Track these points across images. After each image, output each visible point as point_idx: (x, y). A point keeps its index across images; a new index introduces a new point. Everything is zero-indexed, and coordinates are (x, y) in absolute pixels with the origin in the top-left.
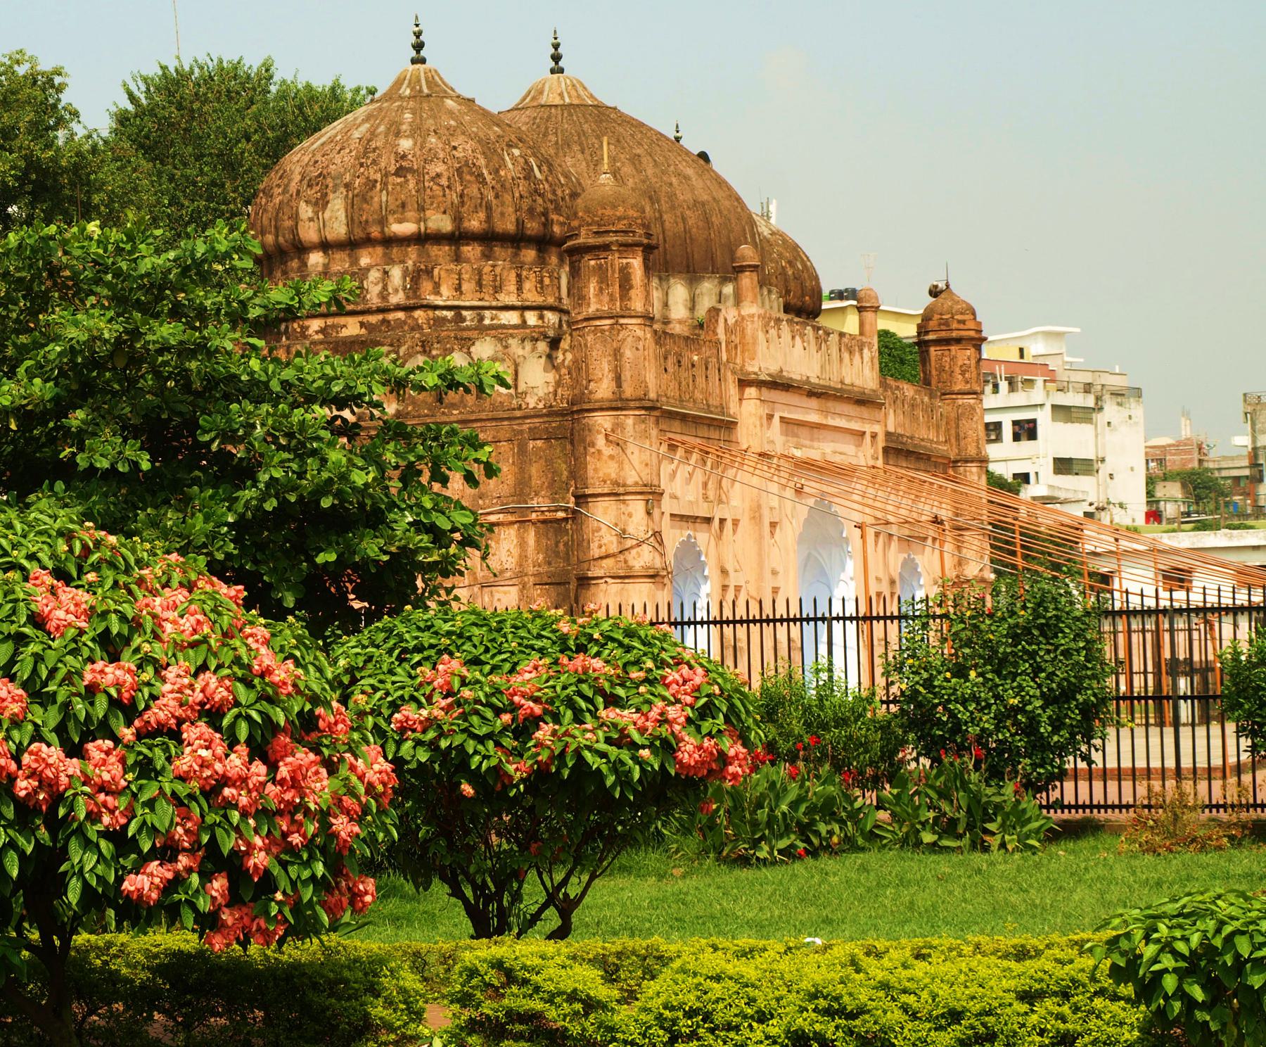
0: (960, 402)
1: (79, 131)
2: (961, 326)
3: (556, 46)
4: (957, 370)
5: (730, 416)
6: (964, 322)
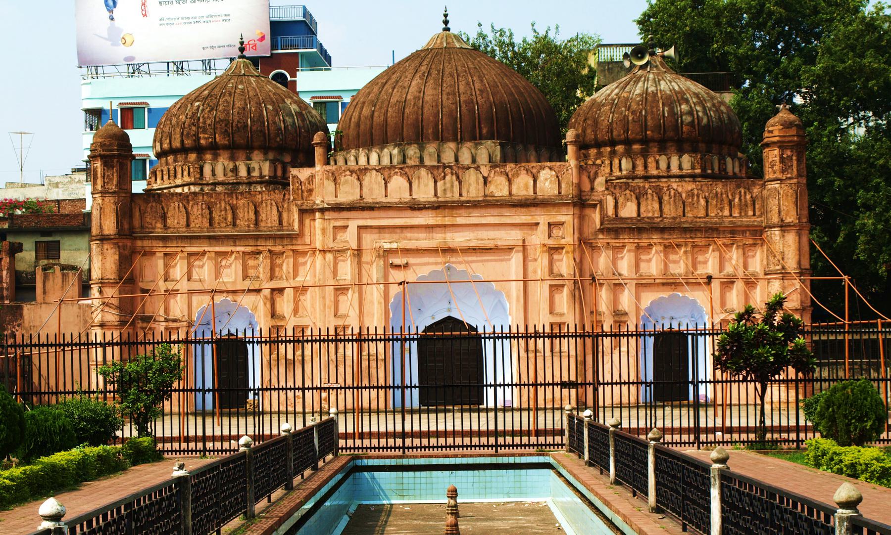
1: (347, 99)
2: (770, 135)
3: (446, 16)
5: (293, 230)
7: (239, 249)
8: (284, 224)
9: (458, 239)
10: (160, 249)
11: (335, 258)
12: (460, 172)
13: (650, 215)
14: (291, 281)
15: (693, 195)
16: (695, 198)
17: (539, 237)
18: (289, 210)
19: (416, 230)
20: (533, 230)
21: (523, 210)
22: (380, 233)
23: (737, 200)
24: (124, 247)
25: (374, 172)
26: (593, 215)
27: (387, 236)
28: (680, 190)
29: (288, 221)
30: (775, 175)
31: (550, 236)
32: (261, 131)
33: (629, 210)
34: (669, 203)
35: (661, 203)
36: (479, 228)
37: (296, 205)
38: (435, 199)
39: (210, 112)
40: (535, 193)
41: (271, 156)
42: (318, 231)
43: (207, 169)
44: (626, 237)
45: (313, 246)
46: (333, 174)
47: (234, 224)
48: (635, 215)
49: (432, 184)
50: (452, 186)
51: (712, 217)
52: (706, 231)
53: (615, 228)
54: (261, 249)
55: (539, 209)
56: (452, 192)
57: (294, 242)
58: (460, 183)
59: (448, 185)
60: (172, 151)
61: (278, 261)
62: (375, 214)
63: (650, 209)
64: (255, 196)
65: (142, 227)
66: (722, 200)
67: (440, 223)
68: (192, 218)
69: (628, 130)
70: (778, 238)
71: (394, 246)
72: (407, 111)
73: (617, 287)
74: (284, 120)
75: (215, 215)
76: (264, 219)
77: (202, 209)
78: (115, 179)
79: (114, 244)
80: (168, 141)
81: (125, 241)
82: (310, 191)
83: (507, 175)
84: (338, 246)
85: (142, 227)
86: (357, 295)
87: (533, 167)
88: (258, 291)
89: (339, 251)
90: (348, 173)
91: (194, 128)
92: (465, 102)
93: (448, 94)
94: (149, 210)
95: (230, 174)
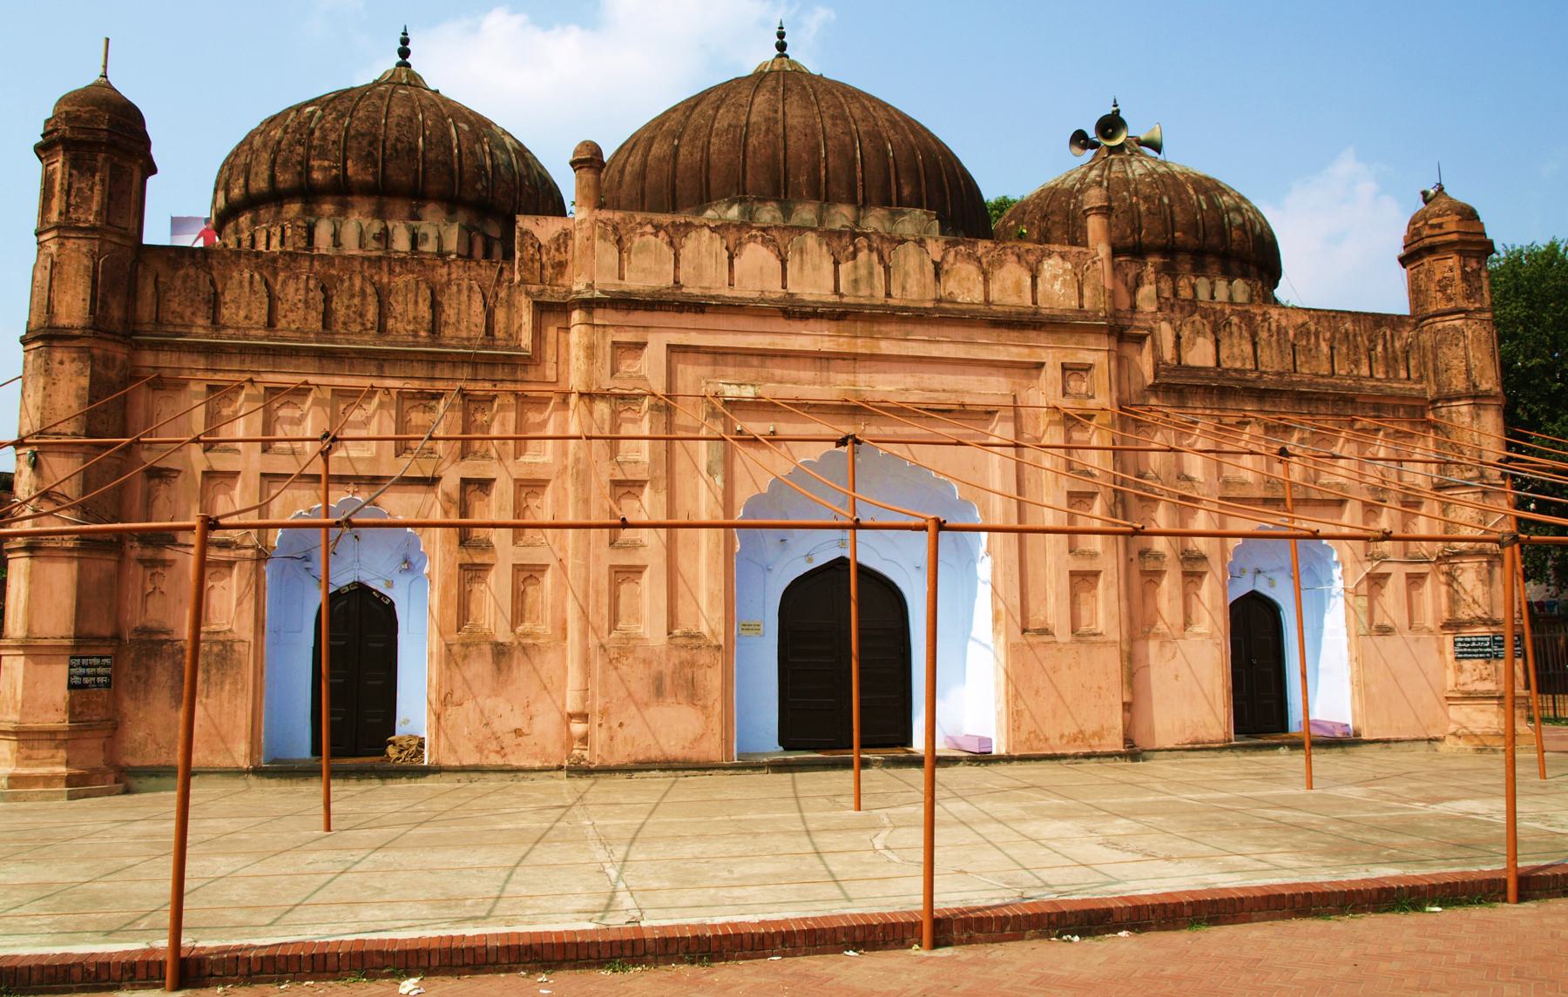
0: (1440, 326)
2: (1437, 231)
3: (781, 35)
4: (1433, 286)
6: (1440, 226)
7: (388, 383)
8: (499, 333)
9: (883, 385)
10: (200, 375)
11: (615, 414)
12: (886, 248)
13: (1238, 365)
14: (509, 462)
15: (1309, 333)
16: (1313, 340)
17: (1043, 392)
18: (510, 304)
19: (793, 361)
20: (1030, 377)
21: (1014, 334)
22: (715, 363)
23: (1380, 348)
24: (108, 362)
25: (706, 231)
26: (1138, 358)
27: (730, 371)
28: (1284, 323)
29: (507, 328)
30: (1453, 304)
31: (1065, 394)
32: (445, 164)
33: (1200, 354)
34: (1270, 344)
35: (1254, 345)
36: (921, 367)
37: (528, 294)
38: (835, 298)
39: (336, 119)
40: (1035, 302)
41: (462, 216)
42: (576, 351)
43: (323, 231)
44: (1198, 404)
45: (561, 387)
46: (615, 229)
47: (382, 329)
48: (1211, 363)
49: (828, 266)
50: (871, 274)
51: (1342, 378)
52: (1334, 402)
53: (1179, 386)
54: (440, 385)
55: (1043, 335)
56: (871, 286)
57: (520, 375)
58: (887, 269)
59: (863, 272)
60: (251, 202)
61: (481, 418)
62: (707, 320)
63: (1237, 355)
64: (434, 268)
65: (158, 321)
66: (1357, 347)
67: (845, 349)
68: (282, 308)
69: (1140, 229)
70: (1468, 420)
71: (748, 392)
72: (753, 141)
73: (1187, 503)
74: (491, 153)
75: (340, 307)
76: (452, 320)
77: (308, 290)
78: (97, 198)
79: (80, 349)
80: (242, 181)
81: (111, 346)
82: (561, 266)
83: (979, 260)
84: (619, 386)
85: (158, 321)
86: (663, 498)
87: (1028, 251)
88: (431, 482)
89: (622, 397)
90: (649, 229)
91: (300, 150)
92: (868, 133)
93: (833, 117)
94: (178, 283)
95: (374, 244)
